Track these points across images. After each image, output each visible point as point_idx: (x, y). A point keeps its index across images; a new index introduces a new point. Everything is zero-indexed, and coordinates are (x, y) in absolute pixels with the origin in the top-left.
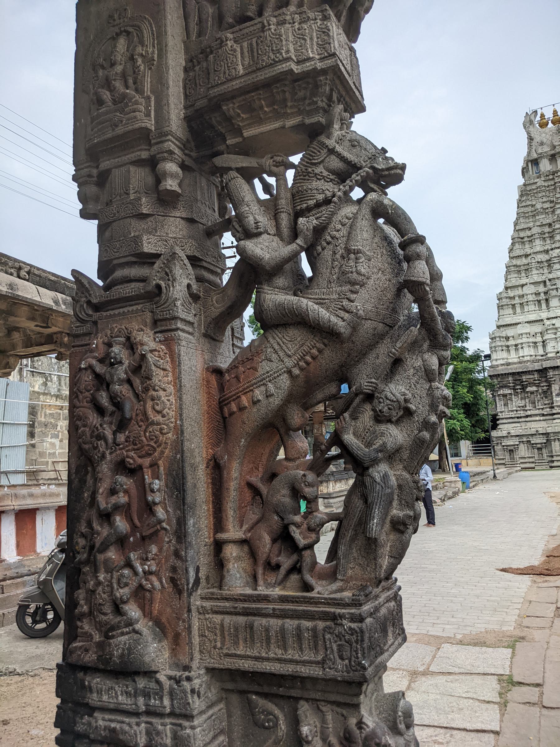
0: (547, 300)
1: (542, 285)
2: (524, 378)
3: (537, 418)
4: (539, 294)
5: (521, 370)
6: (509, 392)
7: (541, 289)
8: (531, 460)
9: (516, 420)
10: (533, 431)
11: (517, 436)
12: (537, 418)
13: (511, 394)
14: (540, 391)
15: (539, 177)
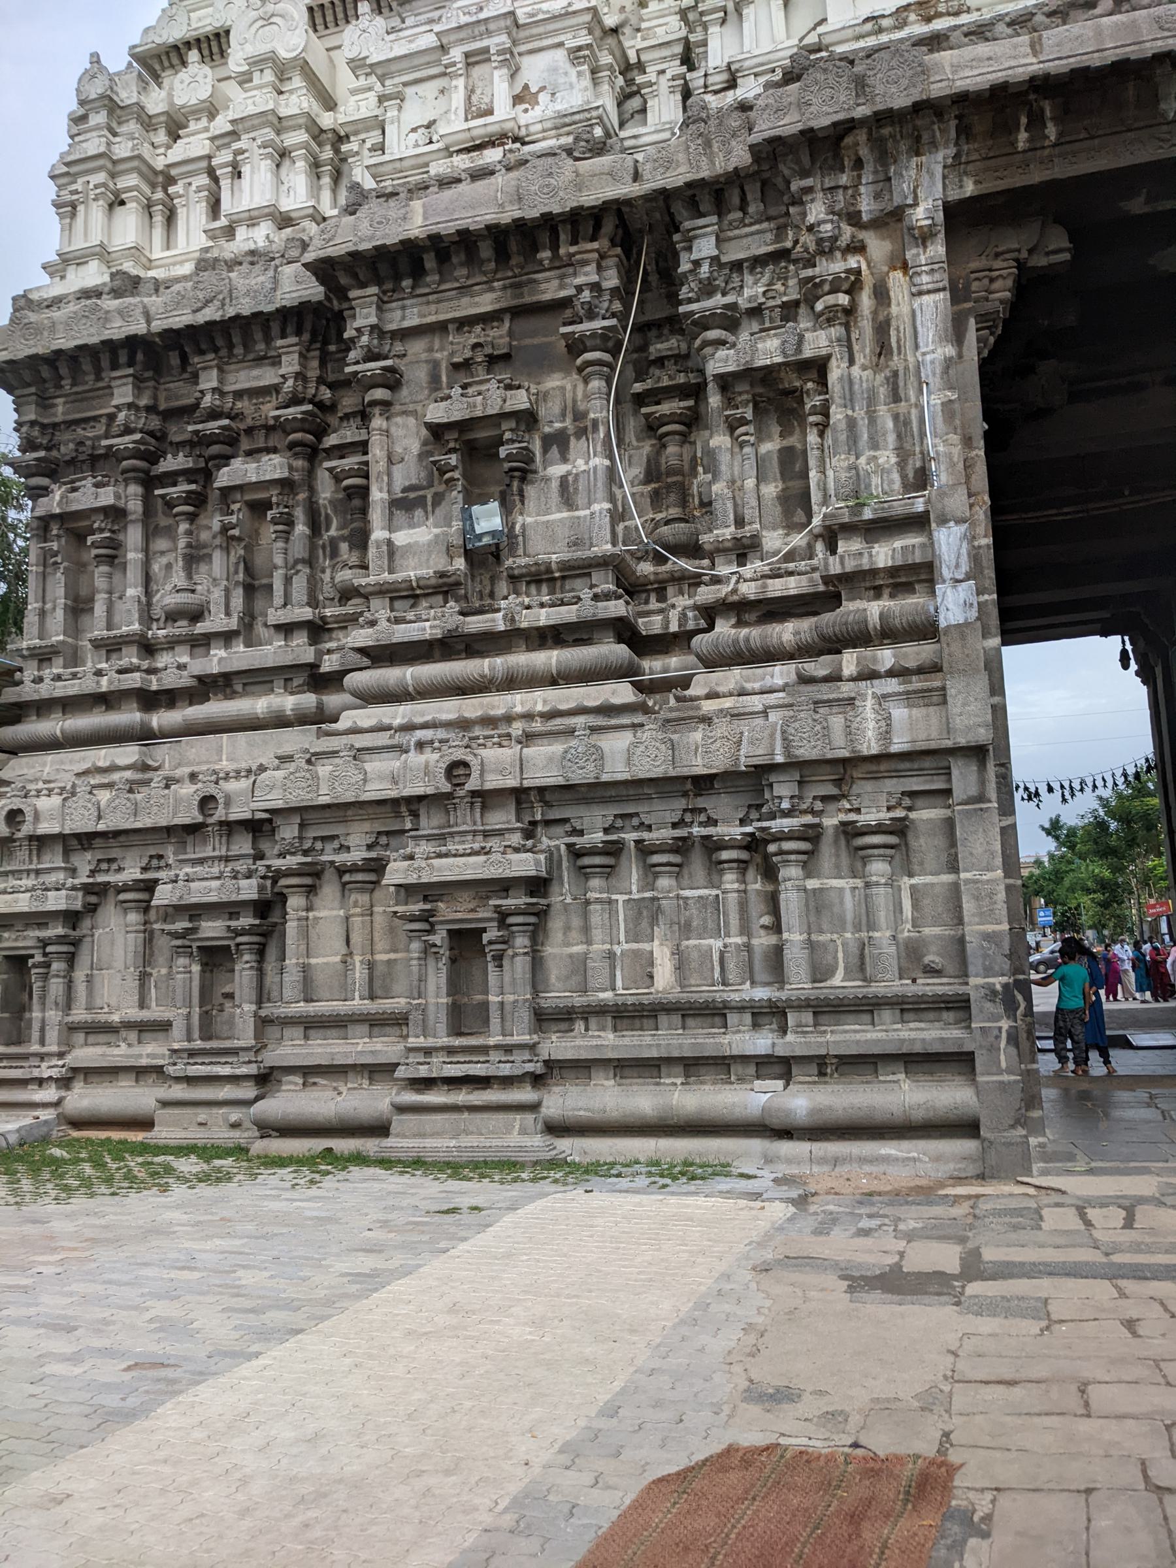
3: (260, 705)
5: (181, 319)
6: (107, 497)
8: (151, 1051)
9: (129, 716)
10: (177, 805)
11: (86, 840)
12: (260, 705)
13: (116, 514)
14: (326, 492)
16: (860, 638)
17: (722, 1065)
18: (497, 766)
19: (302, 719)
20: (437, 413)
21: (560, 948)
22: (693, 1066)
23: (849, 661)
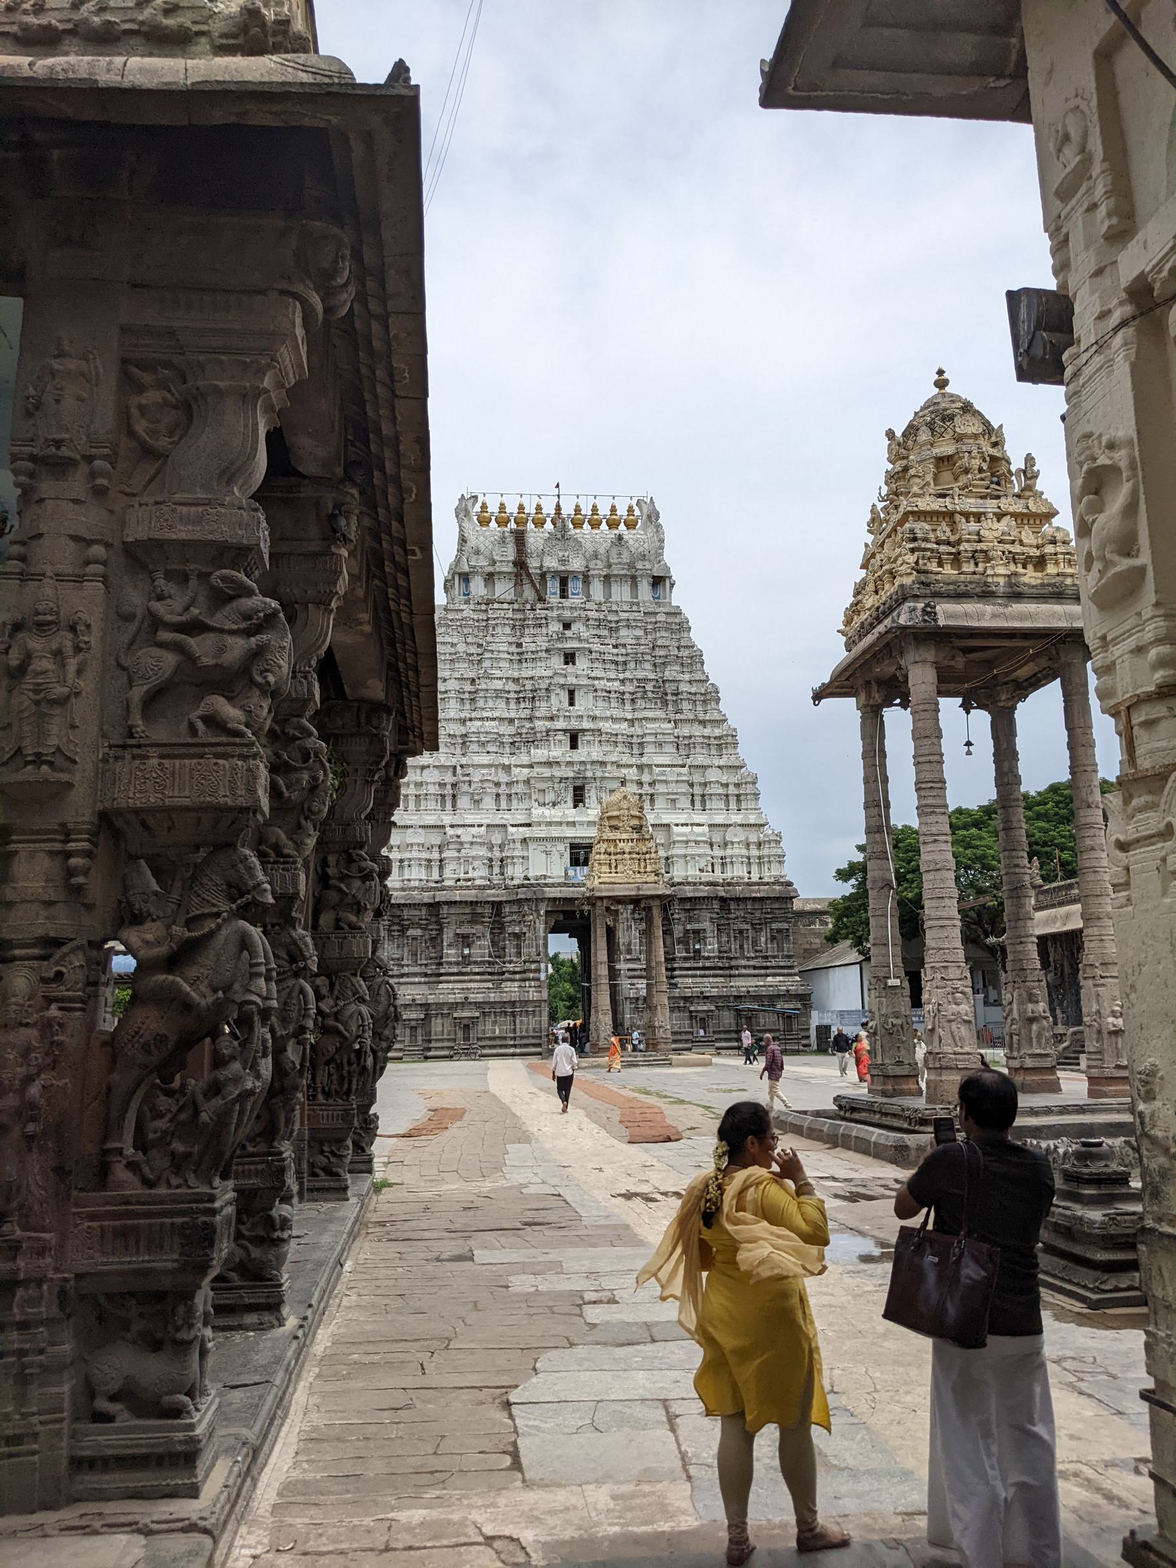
0: (454, 796)
1: (450, 772)
2: (406, 913)
3: (417, 980)
4: (445, 784)
7: (449, 778)
12: (417, 980)
15: (467, 602)
16: (529, 980)
17: (506, 1046)
18: (473, 997)
19: (425, 983)
20: (458, 931)
21: (481, 1028)
22: (501, 1046)
23: (527, 984)
